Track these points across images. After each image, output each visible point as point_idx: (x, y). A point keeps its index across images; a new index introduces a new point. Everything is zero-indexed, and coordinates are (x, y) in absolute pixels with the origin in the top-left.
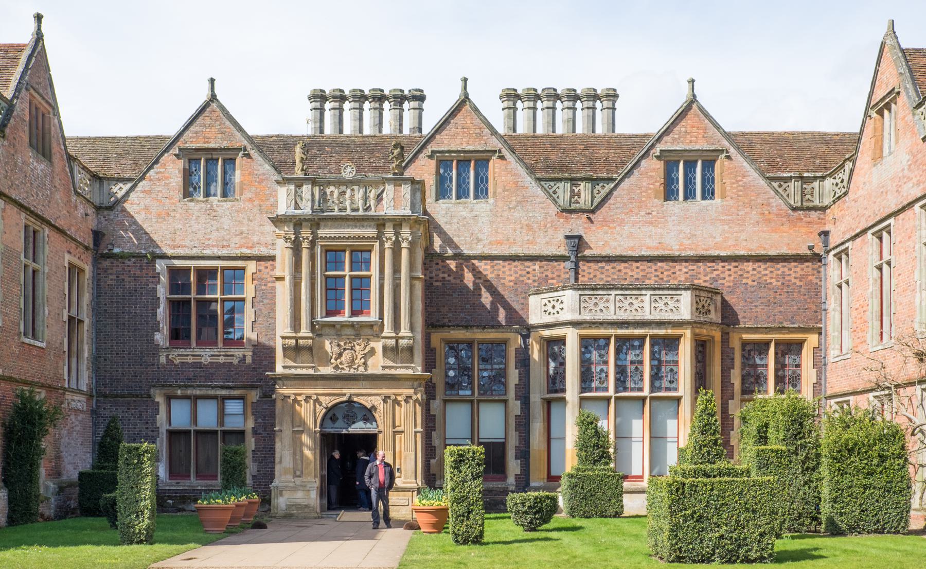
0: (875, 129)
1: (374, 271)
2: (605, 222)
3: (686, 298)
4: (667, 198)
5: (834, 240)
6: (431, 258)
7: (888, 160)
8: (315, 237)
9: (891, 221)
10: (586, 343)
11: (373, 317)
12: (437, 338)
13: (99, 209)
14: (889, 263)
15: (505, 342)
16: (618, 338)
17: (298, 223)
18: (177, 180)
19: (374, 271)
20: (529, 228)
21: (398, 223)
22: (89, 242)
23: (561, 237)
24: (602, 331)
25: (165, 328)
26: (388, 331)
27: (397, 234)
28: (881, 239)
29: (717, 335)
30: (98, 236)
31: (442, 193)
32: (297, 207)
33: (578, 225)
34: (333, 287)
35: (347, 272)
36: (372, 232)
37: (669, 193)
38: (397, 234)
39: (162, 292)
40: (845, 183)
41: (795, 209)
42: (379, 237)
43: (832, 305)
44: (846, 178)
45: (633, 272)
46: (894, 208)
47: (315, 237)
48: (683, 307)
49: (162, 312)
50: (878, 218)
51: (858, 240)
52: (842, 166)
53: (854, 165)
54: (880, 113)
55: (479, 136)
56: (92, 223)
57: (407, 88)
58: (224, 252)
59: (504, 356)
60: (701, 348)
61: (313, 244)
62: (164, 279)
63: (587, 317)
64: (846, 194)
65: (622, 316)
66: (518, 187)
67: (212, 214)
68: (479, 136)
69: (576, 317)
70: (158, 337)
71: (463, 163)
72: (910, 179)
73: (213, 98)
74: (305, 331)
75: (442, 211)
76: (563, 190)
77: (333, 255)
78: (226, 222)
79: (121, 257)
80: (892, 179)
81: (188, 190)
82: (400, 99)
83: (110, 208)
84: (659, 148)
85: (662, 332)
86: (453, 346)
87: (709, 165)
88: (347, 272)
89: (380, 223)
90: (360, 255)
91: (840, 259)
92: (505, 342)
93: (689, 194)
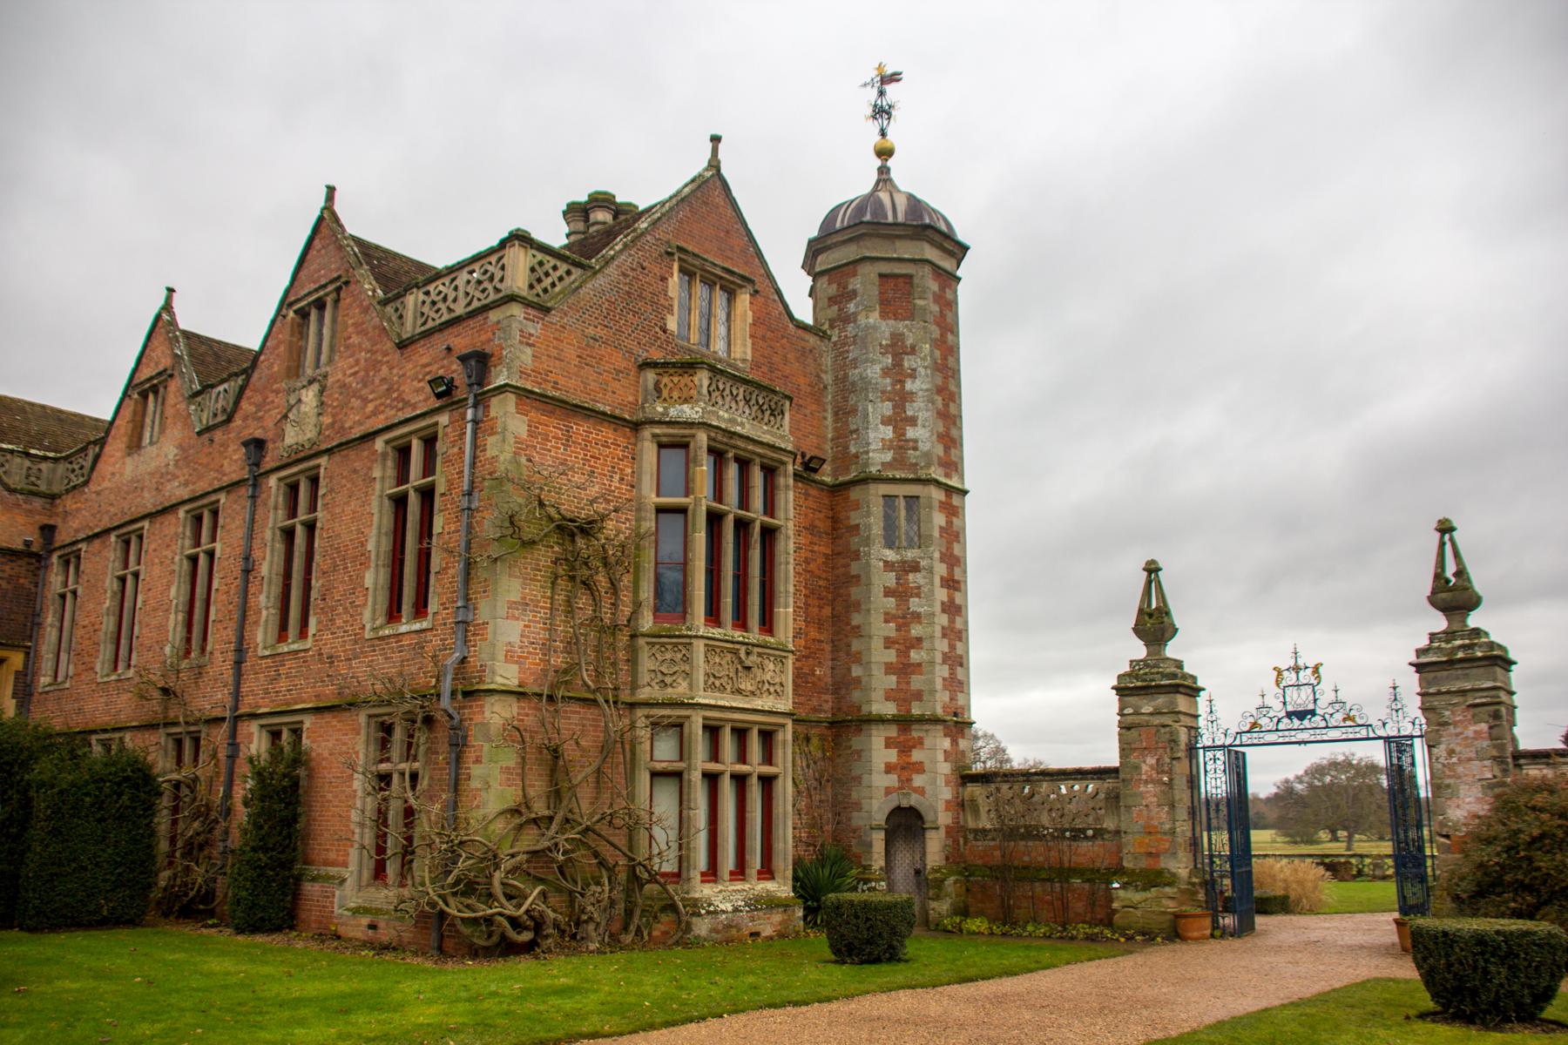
0: (135, 413)
5: (63, 537)
7: (150, 451)
9: (146, 524)
14: (136, 575)
28: (127, 543)
40: (86, 471)
41: (12, 491)
43: (50, 619)
44: (88, 464)
46: (150, 508)
50: (127, 518)
51: (97, 543)
52: (84, 449)
53: (102, 449)
54: (144, 395)
64: (86, 483)
72: (175, 477)
80: (152, 474)
91: (67, 563)
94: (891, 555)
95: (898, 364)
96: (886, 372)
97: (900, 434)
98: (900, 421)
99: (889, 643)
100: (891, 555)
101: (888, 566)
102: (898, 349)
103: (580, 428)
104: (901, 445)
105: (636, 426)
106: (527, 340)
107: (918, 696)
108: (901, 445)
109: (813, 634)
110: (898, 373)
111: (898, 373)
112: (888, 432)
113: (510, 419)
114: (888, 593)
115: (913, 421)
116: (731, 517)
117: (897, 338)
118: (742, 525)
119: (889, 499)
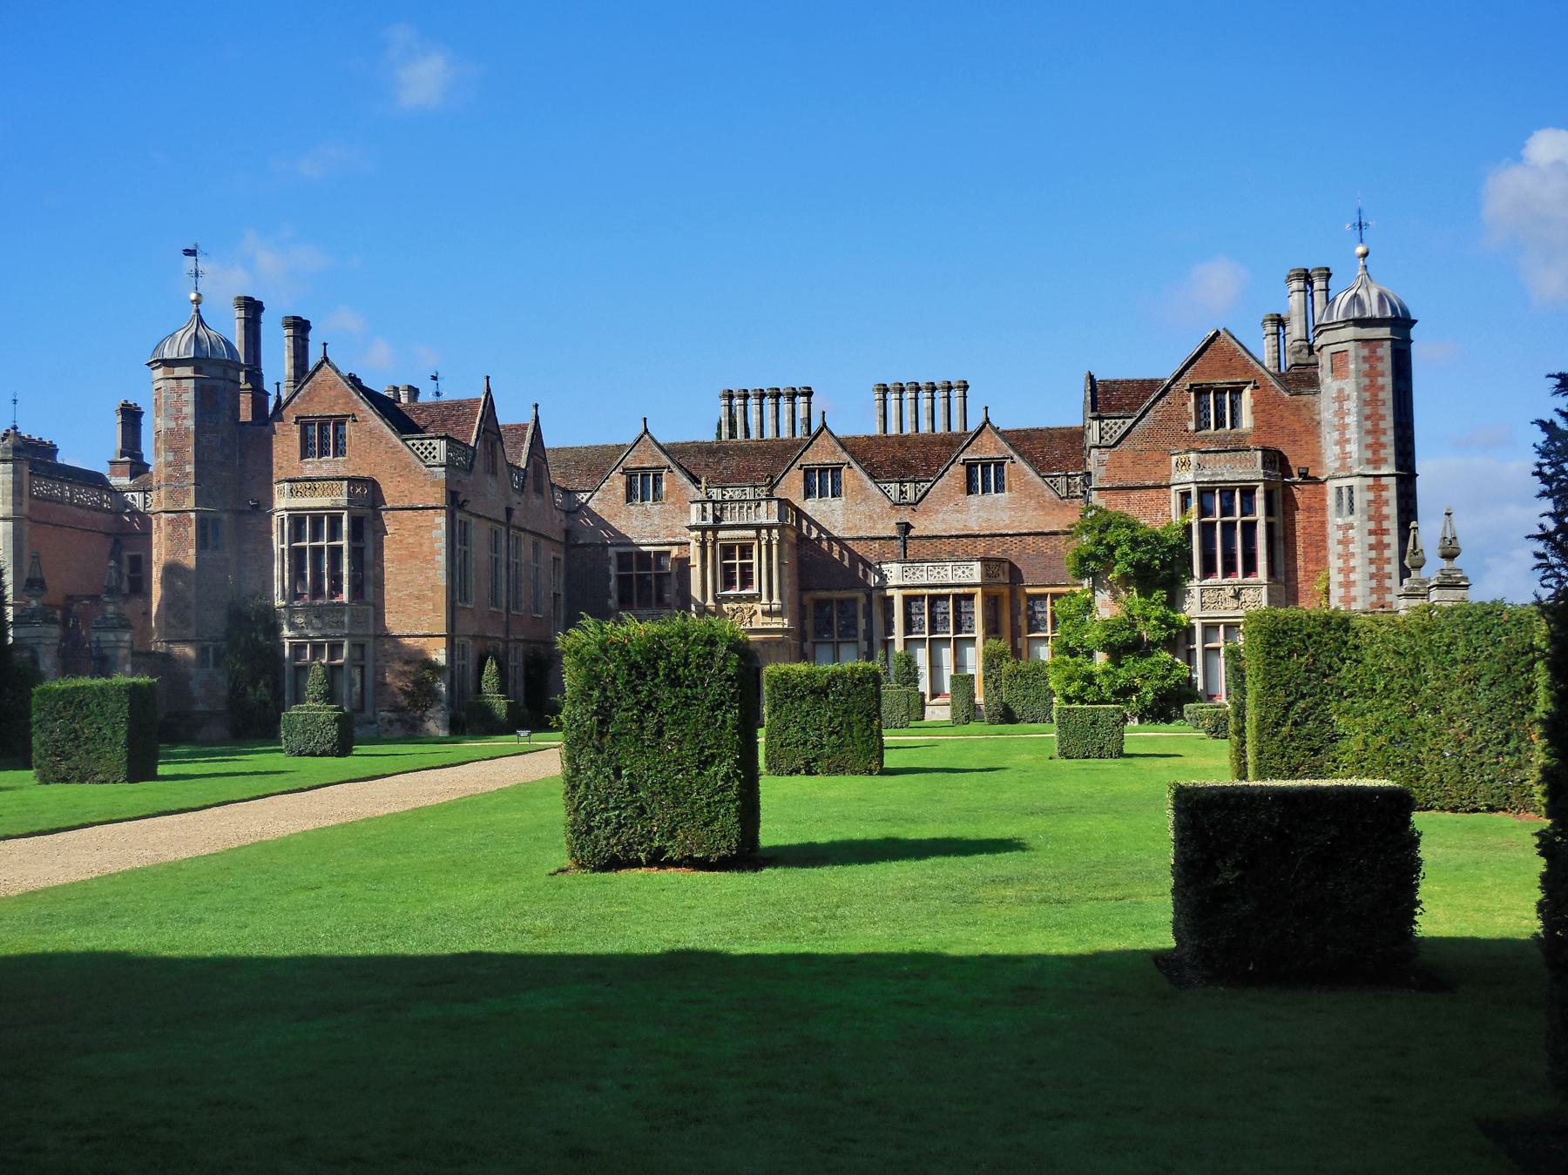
1: (755, 560)
2: (925, 512)
3: (977, 566)
4: (969, 493)
6: (802, 540)
8: (716, 540)
10: (908, 600)
11: (755, 590)
12: (807, 597)
13: (567, 513)
15: (855, 600)
16: (930, 596)
17: (704, 529)
18: (622, 491)
19: (755, 560)
20: (871, 517)
21: (769, 528)
22: (561, 538)
23: (893, 523)
24: (918, 591)
25: (615, 596)
26: (764, 599)
27: (769, 535)
29: (1006, 591)
30: (567, 532)
31: (808, 493)
32: (704, 518)
33: (905, 516)
34: (728, 571)
35: (737, 561)
36: (752, 533)
37: (970, 489)
38: (769, 535)
39: (613, 570)
42: (758, 537)
45: (946, 546)
47: (716, 540)
48: (975, 573)
49: (613, 583)
55: (834, 453)
56: (564, 525)
57: (799, 385)
58: (656, 541)
59: (856, 609)
60: (992, 603)
61: (714, 543)
62: (614, 561)
63: (908, 582)
65: (932, 581)
66: (863, 489)
67: (647, 514)
68: (834, 453)
69: (901, 583)
70: (610, 602)
71: (823, 471)
73: (646, 431)
74: (710, 602)
75: (810, 506)
76: (894, 488)
77: (728, 551)
78: (657, 520)
79: (584, 545)
81: (630, 497)
82: (793, 395)
83: (576, 511)
84: (962, 457)
85: (957, 591)
86: (820, 604)
87: (999, 465)
88: (737, 561)
89: (758, 528)
90: (746, 551)
92: (855, 600)
93: (986, 490)
94: (1340, 521)
95: (1341, 408)
96: (1336, 414)
97: (1343, 448)
98: (1342, 442)
99: (1340, 570)
100: (1340, 521)
101: (1339, 527)
102: (1341, 398)
103: (1135, 495)
104: (1344, 456)
105: (1168, 487)
106: (1101, 463)
107: (1354, 599)
108: (1344, 456)
109: (1311, 567)
110: (1341, 414)
111: (1341, 414)
112: (1337, 449)
113: (1095, 498)
114: (1340, 542)
115: (1348, 441)
116: (1218, 525)
117: (1341, 391)
118: (1228, 528)
119: (1339, 489)
